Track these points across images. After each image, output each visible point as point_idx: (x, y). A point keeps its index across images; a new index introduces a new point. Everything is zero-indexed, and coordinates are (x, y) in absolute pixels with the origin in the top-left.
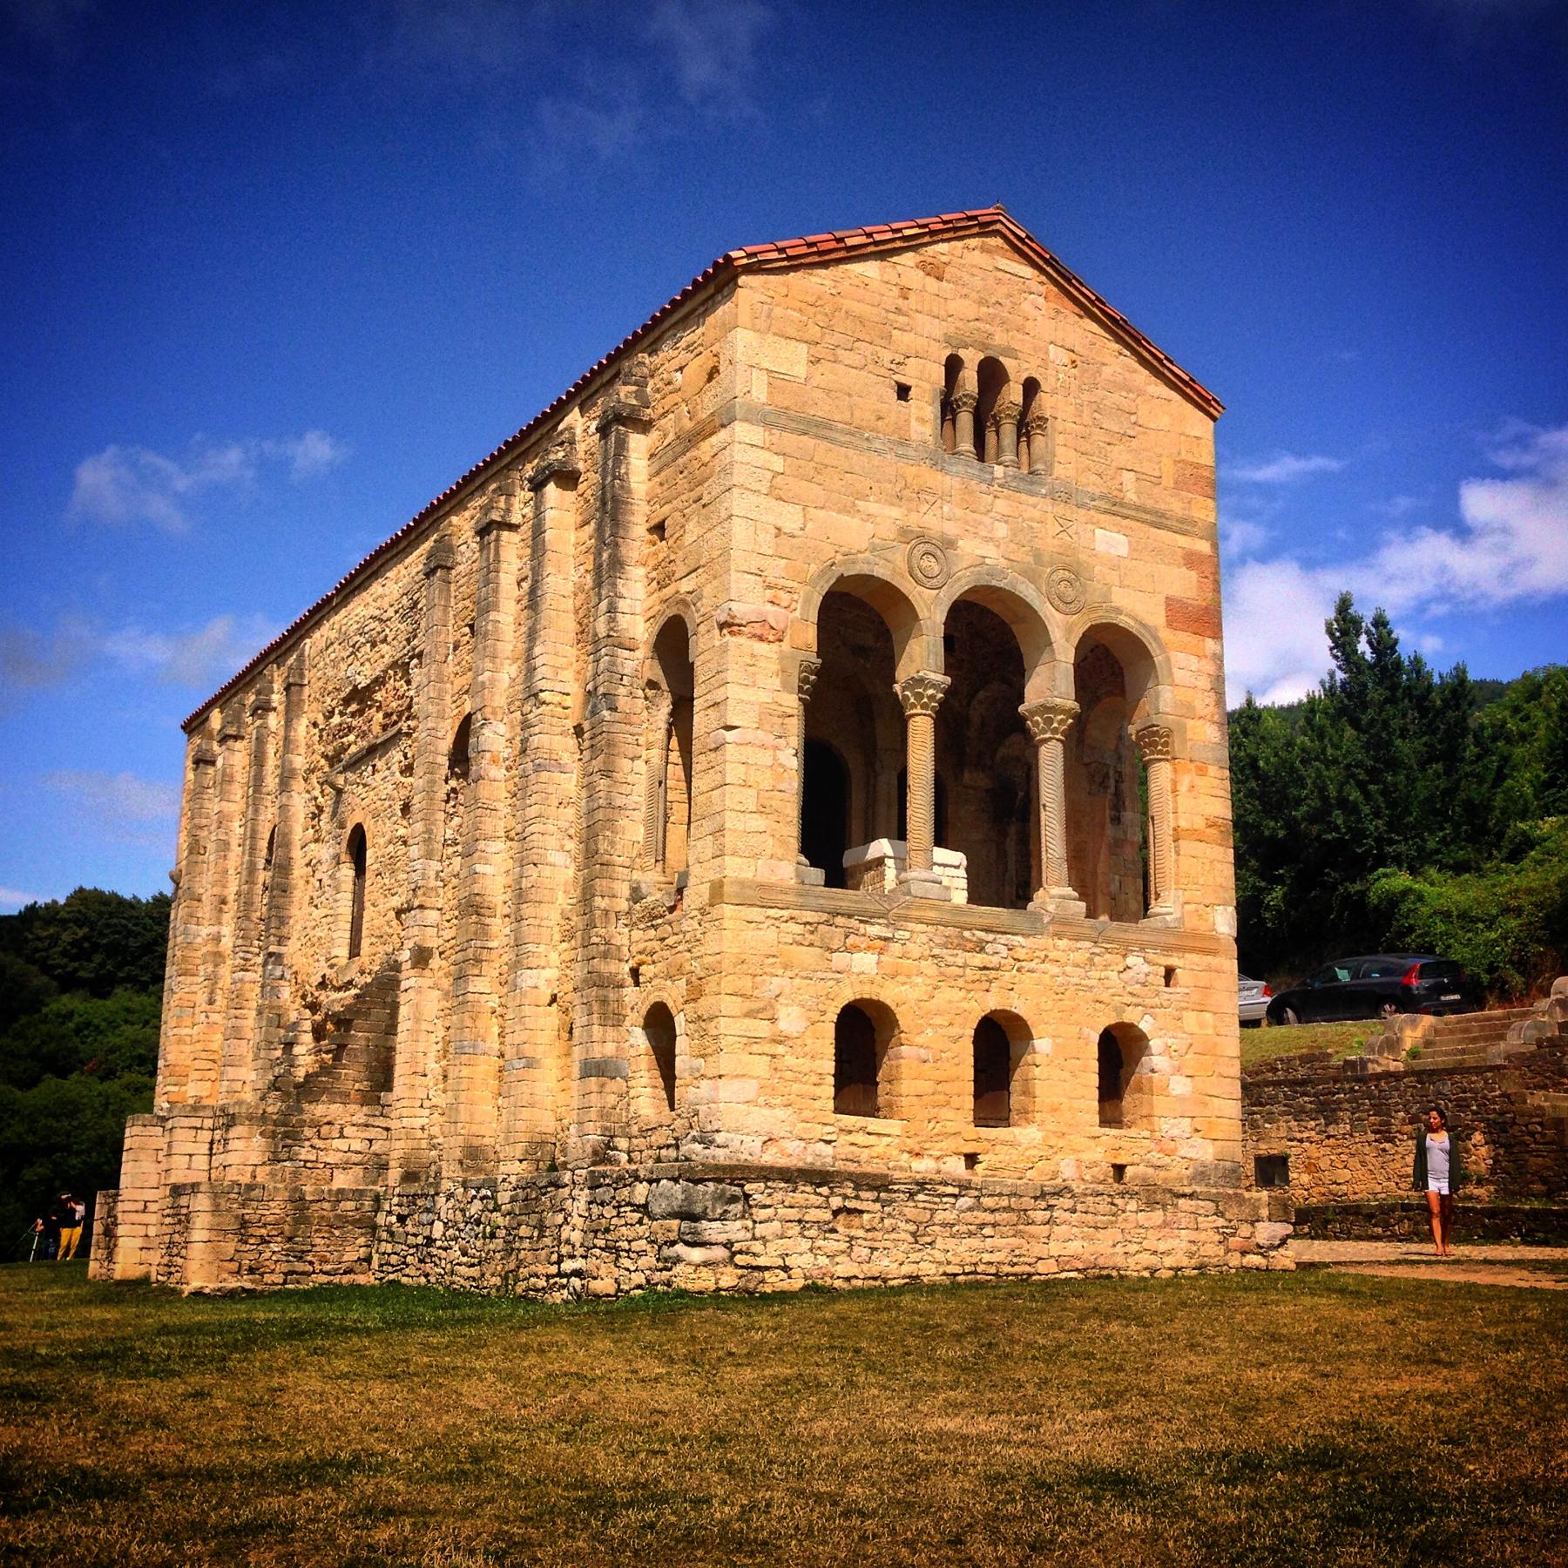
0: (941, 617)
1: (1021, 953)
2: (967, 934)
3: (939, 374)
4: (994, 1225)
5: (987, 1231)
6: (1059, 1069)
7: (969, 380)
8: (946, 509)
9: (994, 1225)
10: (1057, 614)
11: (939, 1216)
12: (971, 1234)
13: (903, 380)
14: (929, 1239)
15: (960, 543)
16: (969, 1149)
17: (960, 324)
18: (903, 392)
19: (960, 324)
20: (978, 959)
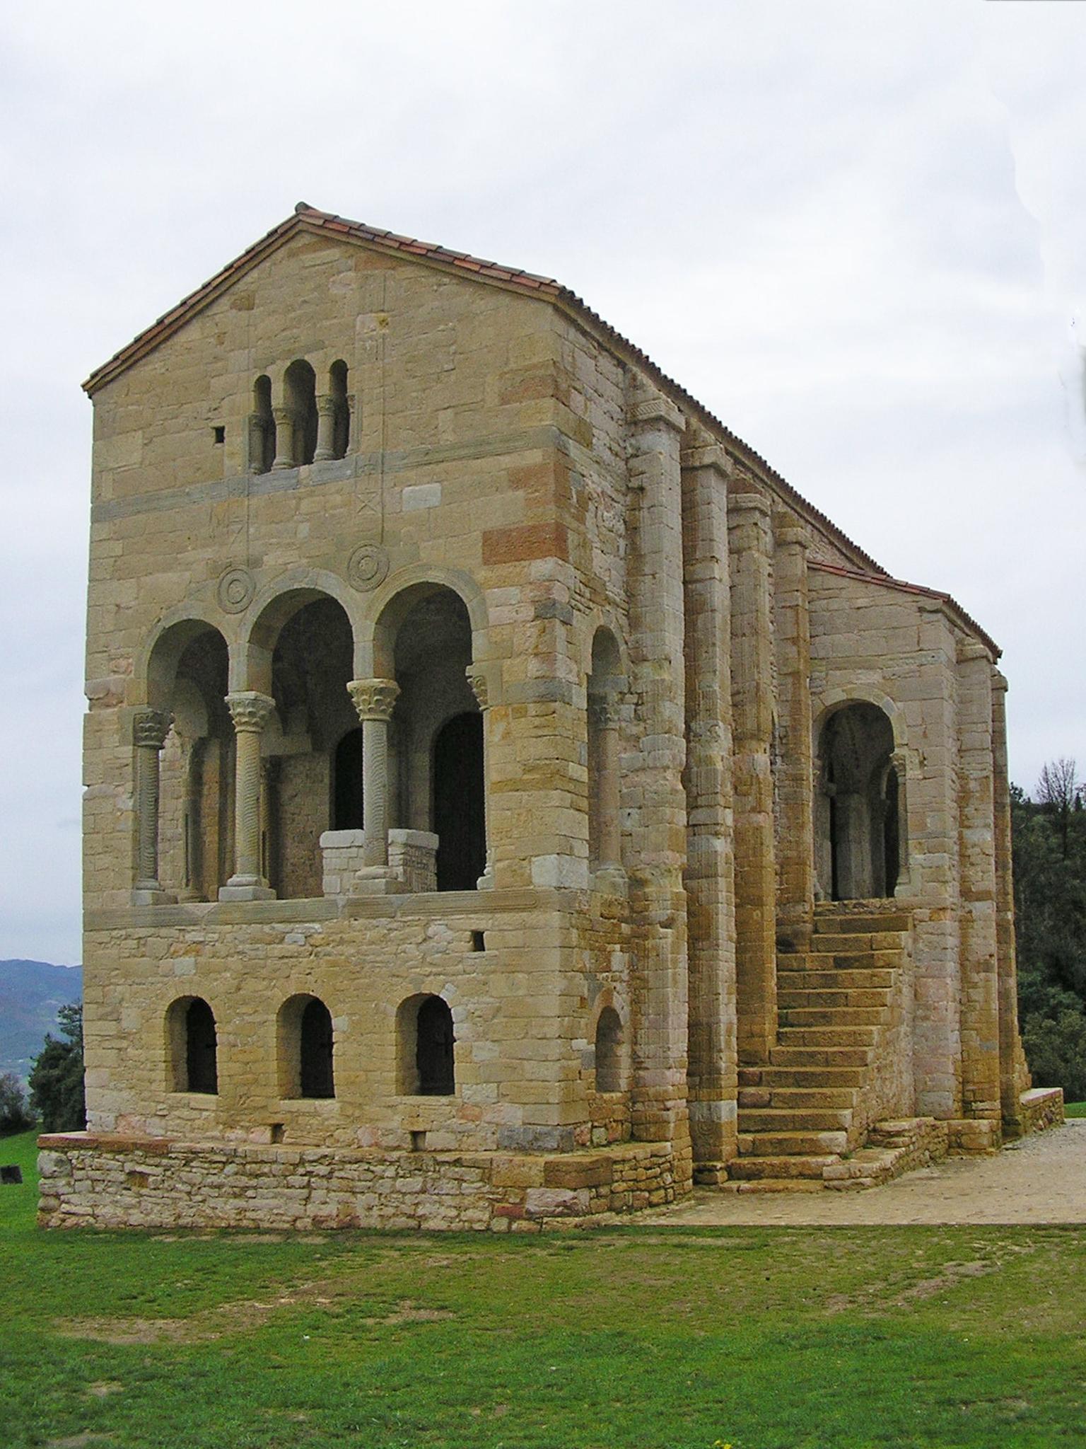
0: (246, 635)
1: (317, 939)
2: (267, 928)
3: (247, 402)
4: (255, 1188)
5: (250, 1193)
6: (367, 1047)
7: (279, 394)
8: (252, 530)
9: (255, 1188)
10: (358, 595)
11: (210, 1179)
12: (235, 1196)
13: (217, 424)
14: (199, 1198)
15: (265, 558)
16: (276, 1119)
17: (267, 343)
18: (220, 434)
19: (267, 343)
20: (277, 949)
